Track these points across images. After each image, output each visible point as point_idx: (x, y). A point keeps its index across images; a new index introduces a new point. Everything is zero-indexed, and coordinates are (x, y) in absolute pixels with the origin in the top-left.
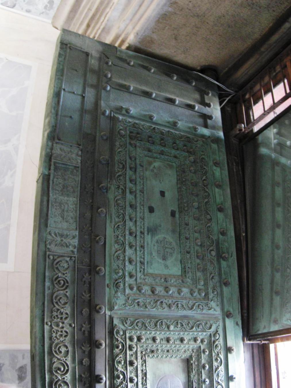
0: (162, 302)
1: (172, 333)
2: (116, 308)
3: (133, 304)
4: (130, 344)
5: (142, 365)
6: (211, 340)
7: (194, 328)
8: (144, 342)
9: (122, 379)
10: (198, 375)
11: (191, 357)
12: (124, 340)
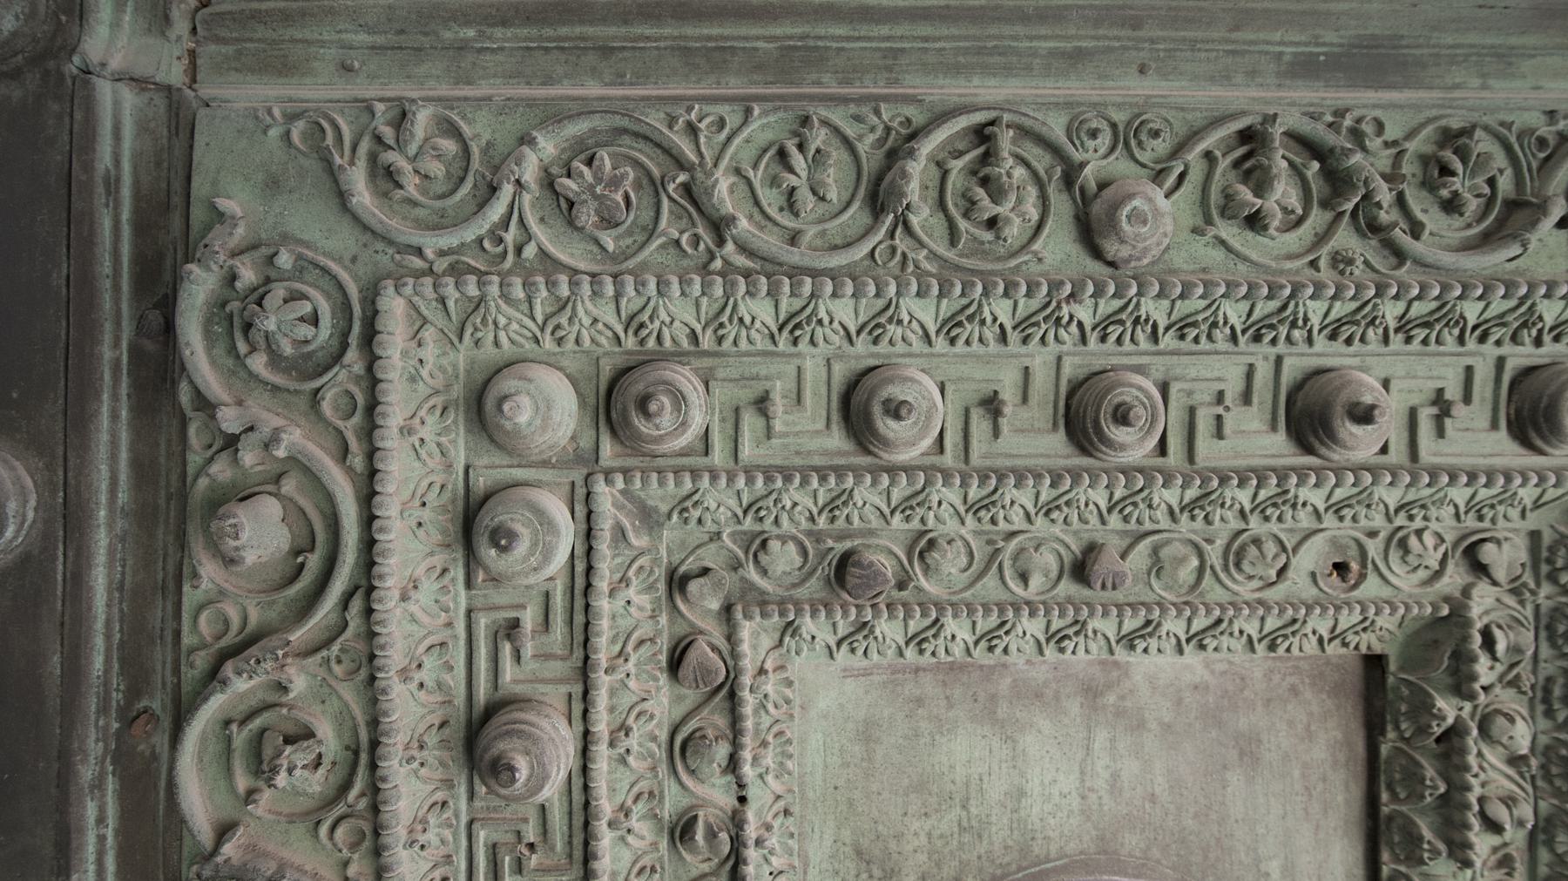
4: (481, 482)
12: (350, 428)
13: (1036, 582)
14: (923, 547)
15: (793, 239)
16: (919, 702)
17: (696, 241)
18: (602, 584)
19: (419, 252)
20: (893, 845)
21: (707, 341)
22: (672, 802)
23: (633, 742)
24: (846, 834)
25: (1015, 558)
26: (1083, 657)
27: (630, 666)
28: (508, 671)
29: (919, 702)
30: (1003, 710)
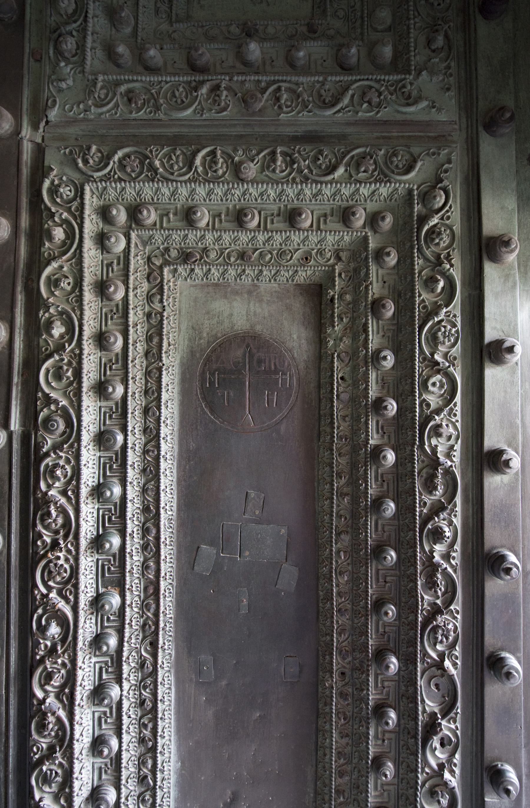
0: (216, 88)
1: (253, 191)
2: (53, 114)
3: (111, 100)
5: (149, 298)
6: (412, 212)
7: (341, 171)
8: (155, 224)
9: (62, 336)
10: (355, 338)
11: (330, 276)
13: (232, 259)
14: (205, 250)
15: (172, 174)
16: (208, 293)
17: (151, 175)
18: (132, 254)
19: (93, 177)
20: (201, 326)
21: (155, 201)
22: (147, 309)
23: (139, 291)
24: (190, 324)
25: (228, 253)
26: (247, 281)
27: (138, 274)
28: (111, 274)
29: (208, 293)
30: (228, 295)
